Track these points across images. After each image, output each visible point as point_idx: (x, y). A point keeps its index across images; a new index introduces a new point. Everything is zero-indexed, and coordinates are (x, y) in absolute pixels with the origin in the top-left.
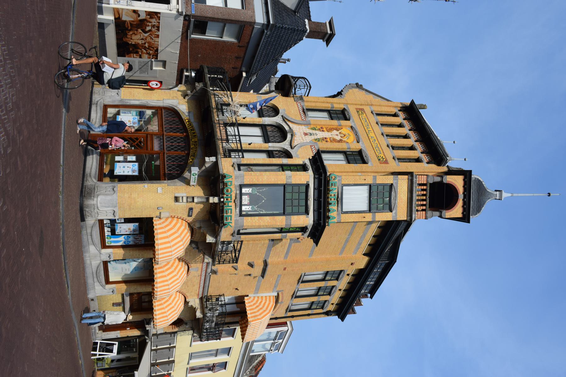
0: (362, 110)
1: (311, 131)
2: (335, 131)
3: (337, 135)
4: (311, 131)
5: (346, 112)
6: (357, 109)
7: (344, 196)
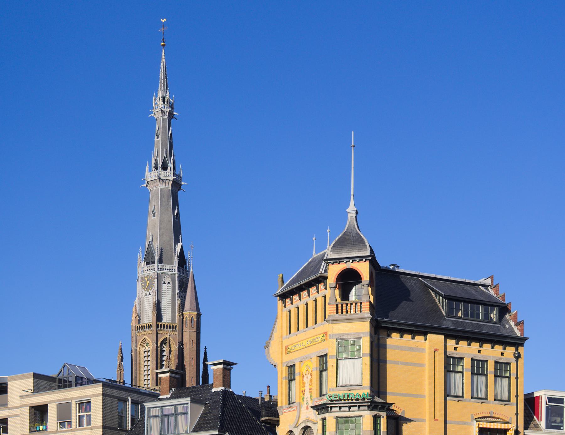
0: (287, 348)
1: (305, 402)
4: (305, 402)
7: (348, 384)
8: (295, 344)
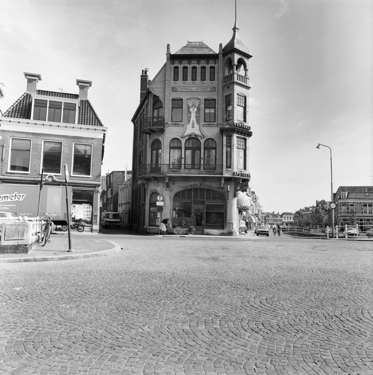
2: (190, 109)
3: (193, 109)
5: (175, 99)
6: (172, 91)
8: (183, 88)
